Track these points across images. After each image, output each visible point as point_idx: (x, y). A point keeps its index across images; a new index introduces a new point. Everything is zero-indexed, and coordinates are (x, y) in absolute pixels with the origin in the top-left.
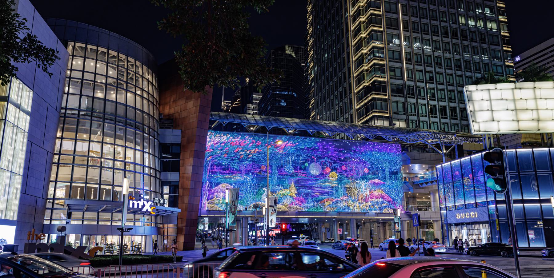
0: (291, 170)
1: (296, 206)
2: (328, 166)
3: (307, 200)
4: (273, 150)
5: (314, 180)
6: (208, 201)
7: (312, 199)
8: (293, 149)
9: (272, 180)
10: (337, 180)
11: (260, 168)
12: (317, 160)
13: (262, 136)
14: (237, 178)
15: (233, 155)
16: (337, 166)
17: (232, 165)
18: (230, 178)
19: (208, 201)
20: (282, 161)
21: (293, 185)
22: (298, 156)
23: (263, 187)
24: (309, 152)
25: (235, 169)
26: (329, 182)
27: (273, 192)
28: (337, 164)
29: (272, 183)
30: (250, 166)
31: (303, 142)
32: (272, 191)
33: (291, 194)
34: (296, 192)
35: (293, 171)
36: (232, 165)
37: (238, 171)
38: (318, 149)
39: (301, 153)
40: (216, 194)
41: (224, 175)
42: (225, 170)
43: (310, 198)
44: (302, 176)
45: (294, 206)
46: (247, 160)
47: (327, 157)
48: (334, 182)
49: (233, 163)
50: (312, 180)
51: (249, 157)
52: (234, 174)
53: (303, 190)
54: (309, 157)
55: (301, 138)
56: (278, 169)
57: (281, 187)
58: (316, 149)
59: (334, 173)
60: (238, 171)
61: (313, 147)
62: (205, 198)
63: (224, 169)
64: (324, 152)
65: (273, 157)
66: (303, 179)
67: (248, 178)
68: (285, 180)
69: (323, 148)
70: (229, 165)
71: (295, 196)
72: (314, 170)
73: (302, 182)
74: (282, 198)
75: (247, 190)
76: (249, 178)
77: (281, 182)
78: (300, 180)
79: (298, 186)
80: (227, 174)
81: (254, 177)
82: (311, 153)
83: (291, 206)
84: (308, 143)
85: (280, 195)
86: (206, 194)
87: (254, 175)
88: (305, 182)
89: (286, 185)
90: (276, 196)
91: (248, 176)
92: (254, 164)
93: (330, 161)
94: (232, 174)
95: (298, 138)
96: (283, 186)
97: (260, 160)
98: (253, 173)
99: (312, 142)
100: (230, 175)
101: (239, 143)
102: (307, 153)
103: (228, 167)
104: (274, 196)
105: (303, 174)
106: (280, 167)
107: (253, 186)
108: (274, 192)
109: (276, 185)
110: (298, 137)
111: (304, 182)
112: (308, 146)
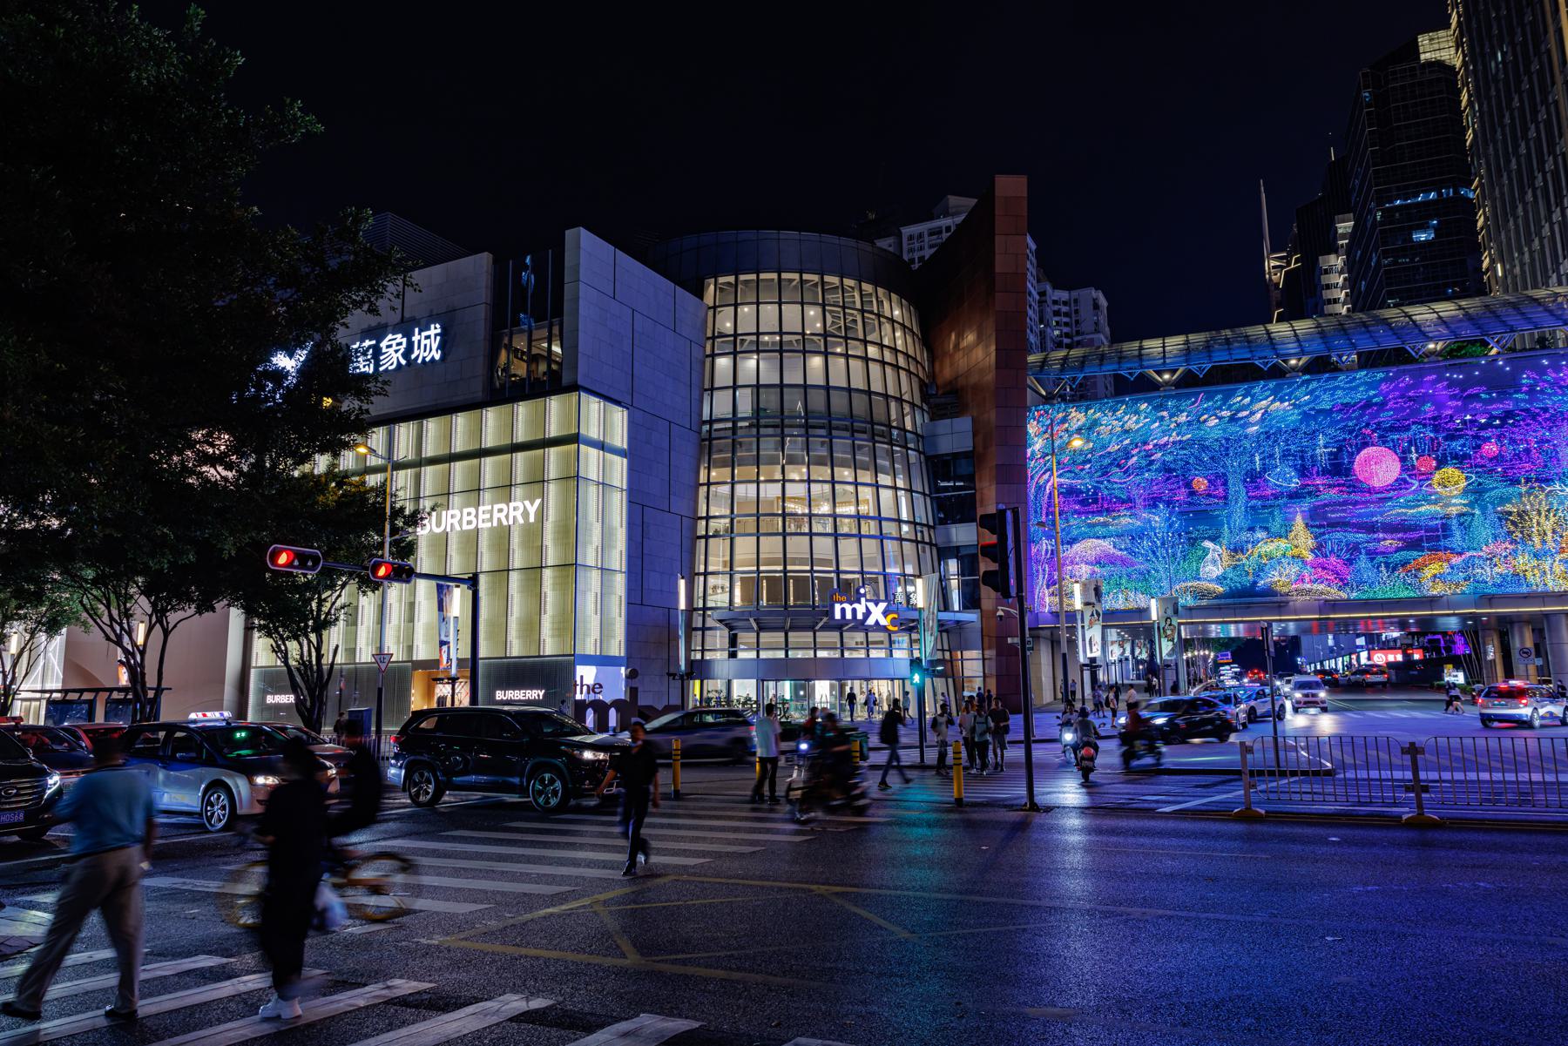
0: (1291, 482)
1: (1315, 586)
2: (1423, 451)
3: (1351, 564)
4: (1224, 430)
5: (1373, 502)
6: (1048, 588)
7: (1372, 560)
8: (1293, 418)
9: (1229, 516)
10: (1465, 492)
11: (1188, 485)
12: (1380, 437)
13: (1188, 396)
14: (1125, 521)
15: (1107, 461)
16: (1463, 445)
17: (1106, 487)
18: (1105, 524)
19: (1048, 588)
20: (1257, 458)
21: (1299, 522)
22: (1313, 435)
23: (1205, 538)
24: (1350, 419)
25: (1116, 497)
26: (1430, 502)
27: (1235, 550)
28: (1462, 441)
29: (1228, 524)
30: (1157, 484)
31: (1325, 391)
32: (1232, 547)
33: (1296, 552)
34: (1311, 543)
35: (1295, 483)
36: (1106, 487)
37: (1123, 502)
38: (1382, 406)
39: (1320, 424)
40: (1070, 568)
41: (1087, 518)
42: (1090, 504)
43: (1363, 557)
44: (1331, 495)
45: (1309, 586)
46: (1149, 470)
47: (1419, 424)
48: (1454, 501)
49: (1109, 481)
50: (1368, 502)
51: (1154, 461)
52: (1114, 511)
53: (1339, 535)
54: (1350, 433)
55: (1319, 380)
56: (1245, 481)
57: (1260, 534)
58: (1376, 404)
59: (1450, 471)
60: (1123, 502)
61: (1361, 400)
62: (1041, 581)
63: (1083, 503)
64: (1404, 409)
65: (1227, 449)
66: (1335, 504)
67: (1158, 519)
68: (1271, 513)
69: (1402, 396)
70: (1094, 487)
71: (1310, 557)
72: (1380, 466)
73: (1333, 512)
74: (1266, 565)
75: (1154, 553)
76: (1157, 518)
77: (1258, 520)
78: (1326, 505)
79: (1317, 527)
80: (1093, 512)
81: (1171, 513)
82: (1357, 418)
83: (1300, 586)
84: (1344, 389)
85: (1260, 556)
86: (1044, 570)
87: (1174, 507)
88: (1344, 511)
89: (1276, 526)
90: (1245, 561)
91: (1154, 513)
92: (1168, 479)
93: (1432, 435)
94: (1109, 511)
95: (1308, 382)
96: (1266, 529)
97: (1188, 463)
98: (1168, 503)
99: (1361, 384)
100: (1102, 516)
101: (1122, 426)
102: (1342, 420)
103: (1095, 493)
104: (1239, 560)
105: (1330, 486)
106: (1254, 479)
107: (1173, 536)
108: (1237, 549)
109: (1241, 529)
110: (1307, 377)
111: (1338, 511)
112: (1345, 401)
